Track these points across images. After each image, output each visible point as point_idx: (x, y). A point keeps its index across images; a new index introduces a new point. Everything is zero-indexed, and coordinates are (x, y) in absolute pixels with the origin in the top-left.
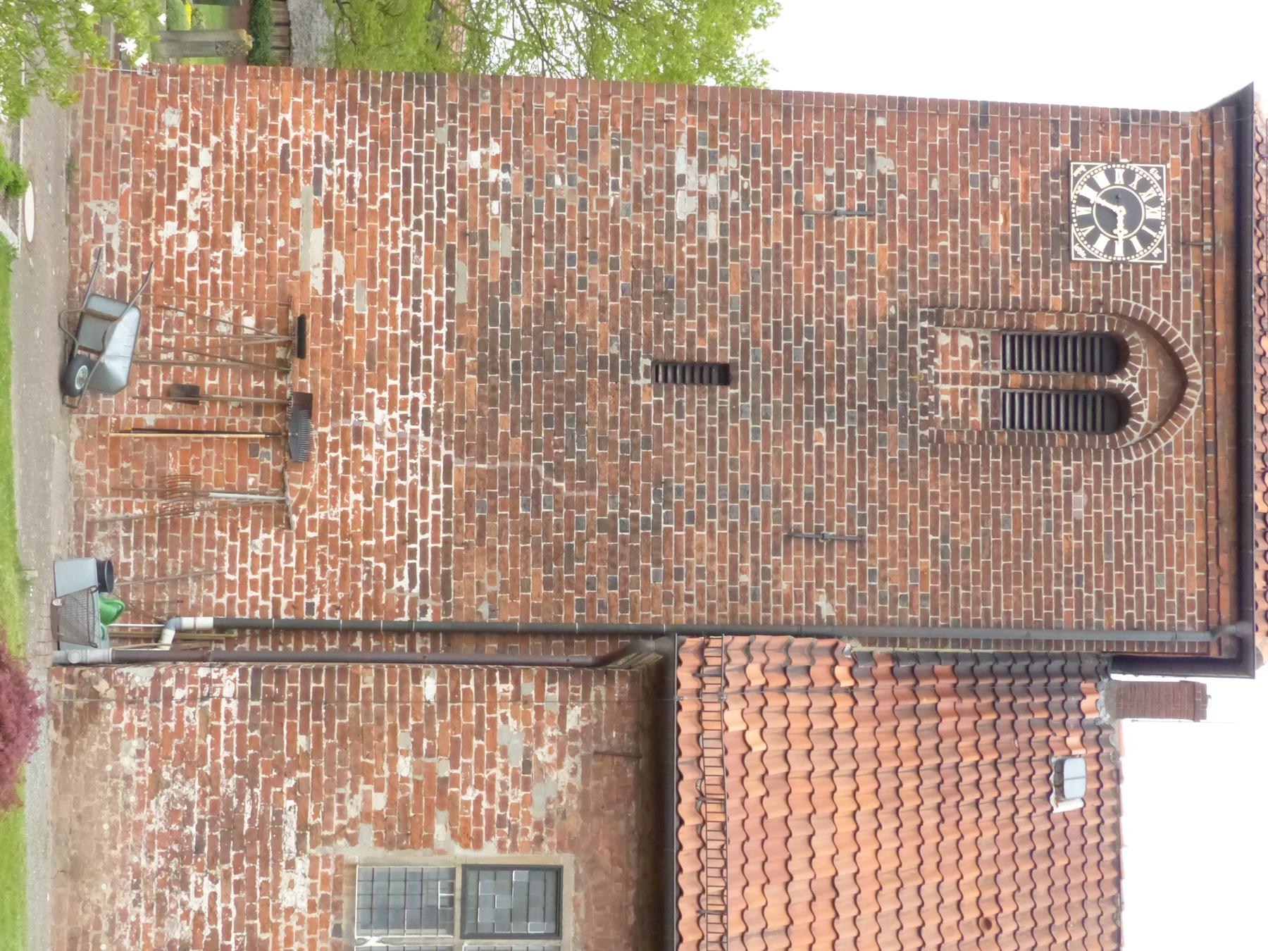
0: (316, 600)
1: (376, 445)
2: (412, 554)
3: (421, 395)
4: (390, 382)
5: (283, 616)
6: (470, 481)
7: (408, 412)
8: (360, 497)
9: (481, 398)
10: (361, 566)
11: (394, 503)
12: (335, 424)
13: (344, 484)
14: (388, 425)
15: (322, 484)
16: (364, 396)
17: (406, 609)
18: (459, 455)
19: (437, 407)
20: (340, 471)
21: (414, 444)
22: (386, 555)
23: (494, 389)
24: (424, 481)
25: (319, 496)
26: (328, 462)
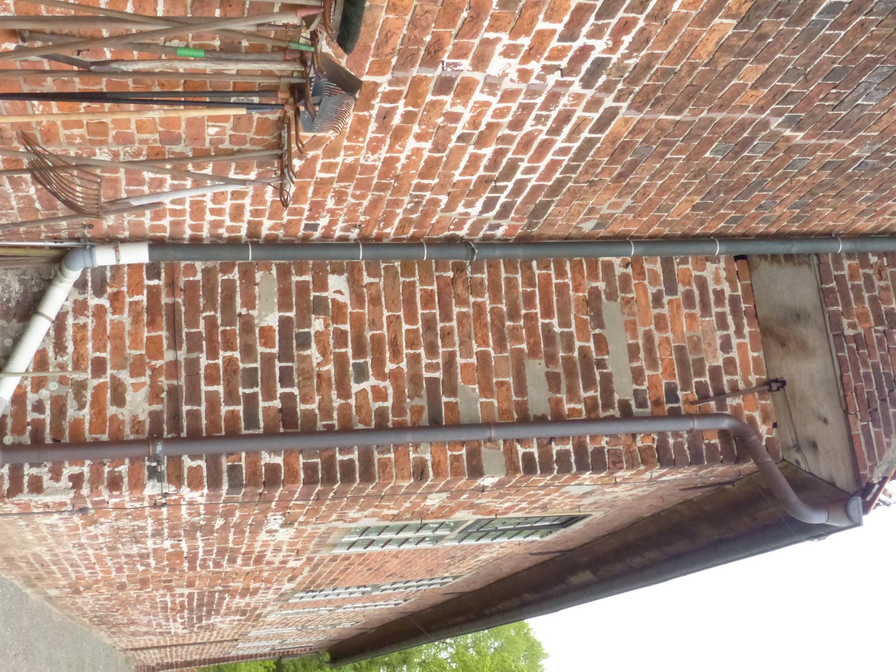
0: (323, 222)
1: (478, 96)
2: (496, 189)
3: (600, 46)
4: (542, 25)
5: (264, 231)
6: (635, 131)
7: (564, 63)
8: (427, 145)
9: (723, 48)
10: (407, 199)
11: (488, 152)
12: (400, 74)
13: (399, 135)
14: (514, 75)
15: (358, 131)
16: (476, 42)
17: (467, 226)
18: (636, 106)
19: (628, 56)
20: (396, 120)
21: (553, 97)
22: (450, 190)
23: (762, 37)
24: (555, 131)
25: (345, 143)
26: (374, 112)
